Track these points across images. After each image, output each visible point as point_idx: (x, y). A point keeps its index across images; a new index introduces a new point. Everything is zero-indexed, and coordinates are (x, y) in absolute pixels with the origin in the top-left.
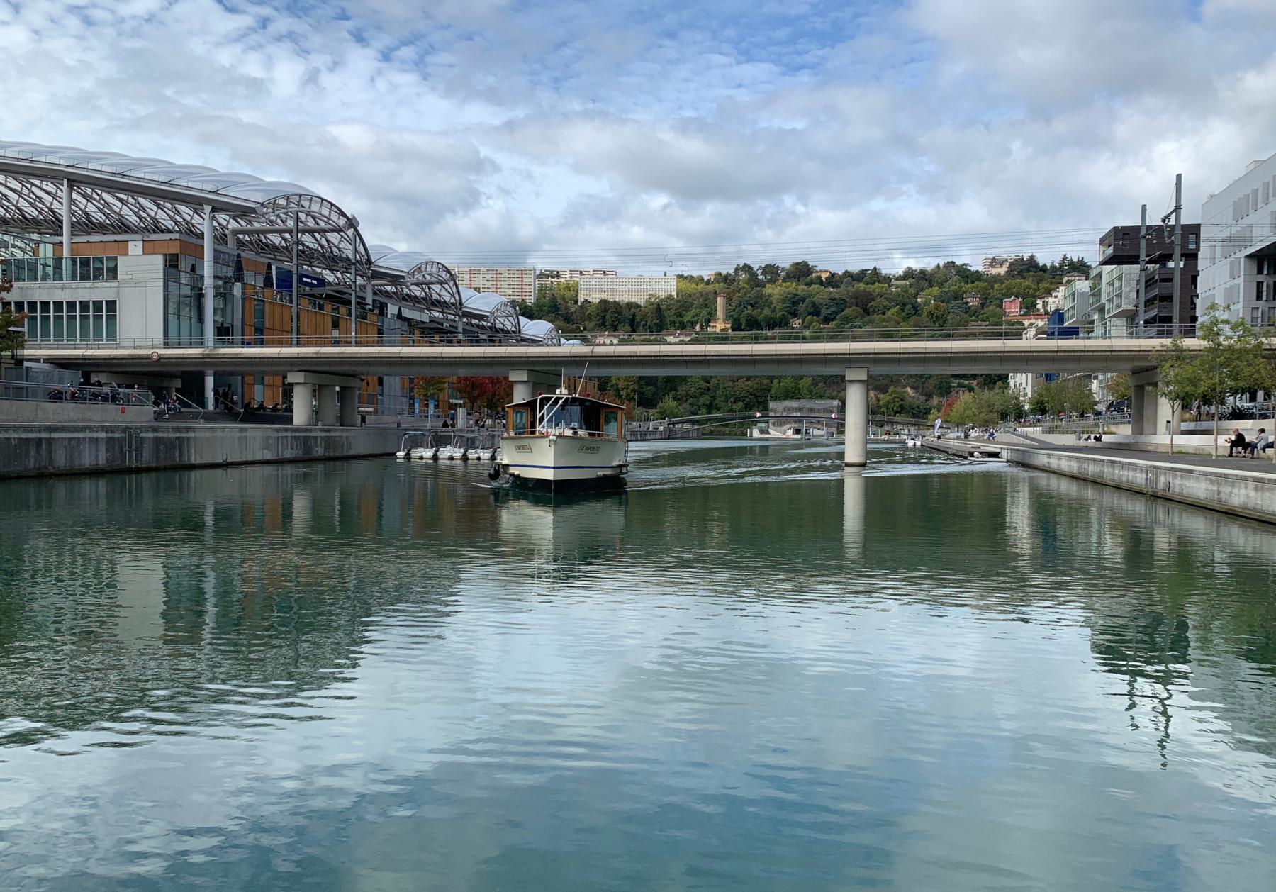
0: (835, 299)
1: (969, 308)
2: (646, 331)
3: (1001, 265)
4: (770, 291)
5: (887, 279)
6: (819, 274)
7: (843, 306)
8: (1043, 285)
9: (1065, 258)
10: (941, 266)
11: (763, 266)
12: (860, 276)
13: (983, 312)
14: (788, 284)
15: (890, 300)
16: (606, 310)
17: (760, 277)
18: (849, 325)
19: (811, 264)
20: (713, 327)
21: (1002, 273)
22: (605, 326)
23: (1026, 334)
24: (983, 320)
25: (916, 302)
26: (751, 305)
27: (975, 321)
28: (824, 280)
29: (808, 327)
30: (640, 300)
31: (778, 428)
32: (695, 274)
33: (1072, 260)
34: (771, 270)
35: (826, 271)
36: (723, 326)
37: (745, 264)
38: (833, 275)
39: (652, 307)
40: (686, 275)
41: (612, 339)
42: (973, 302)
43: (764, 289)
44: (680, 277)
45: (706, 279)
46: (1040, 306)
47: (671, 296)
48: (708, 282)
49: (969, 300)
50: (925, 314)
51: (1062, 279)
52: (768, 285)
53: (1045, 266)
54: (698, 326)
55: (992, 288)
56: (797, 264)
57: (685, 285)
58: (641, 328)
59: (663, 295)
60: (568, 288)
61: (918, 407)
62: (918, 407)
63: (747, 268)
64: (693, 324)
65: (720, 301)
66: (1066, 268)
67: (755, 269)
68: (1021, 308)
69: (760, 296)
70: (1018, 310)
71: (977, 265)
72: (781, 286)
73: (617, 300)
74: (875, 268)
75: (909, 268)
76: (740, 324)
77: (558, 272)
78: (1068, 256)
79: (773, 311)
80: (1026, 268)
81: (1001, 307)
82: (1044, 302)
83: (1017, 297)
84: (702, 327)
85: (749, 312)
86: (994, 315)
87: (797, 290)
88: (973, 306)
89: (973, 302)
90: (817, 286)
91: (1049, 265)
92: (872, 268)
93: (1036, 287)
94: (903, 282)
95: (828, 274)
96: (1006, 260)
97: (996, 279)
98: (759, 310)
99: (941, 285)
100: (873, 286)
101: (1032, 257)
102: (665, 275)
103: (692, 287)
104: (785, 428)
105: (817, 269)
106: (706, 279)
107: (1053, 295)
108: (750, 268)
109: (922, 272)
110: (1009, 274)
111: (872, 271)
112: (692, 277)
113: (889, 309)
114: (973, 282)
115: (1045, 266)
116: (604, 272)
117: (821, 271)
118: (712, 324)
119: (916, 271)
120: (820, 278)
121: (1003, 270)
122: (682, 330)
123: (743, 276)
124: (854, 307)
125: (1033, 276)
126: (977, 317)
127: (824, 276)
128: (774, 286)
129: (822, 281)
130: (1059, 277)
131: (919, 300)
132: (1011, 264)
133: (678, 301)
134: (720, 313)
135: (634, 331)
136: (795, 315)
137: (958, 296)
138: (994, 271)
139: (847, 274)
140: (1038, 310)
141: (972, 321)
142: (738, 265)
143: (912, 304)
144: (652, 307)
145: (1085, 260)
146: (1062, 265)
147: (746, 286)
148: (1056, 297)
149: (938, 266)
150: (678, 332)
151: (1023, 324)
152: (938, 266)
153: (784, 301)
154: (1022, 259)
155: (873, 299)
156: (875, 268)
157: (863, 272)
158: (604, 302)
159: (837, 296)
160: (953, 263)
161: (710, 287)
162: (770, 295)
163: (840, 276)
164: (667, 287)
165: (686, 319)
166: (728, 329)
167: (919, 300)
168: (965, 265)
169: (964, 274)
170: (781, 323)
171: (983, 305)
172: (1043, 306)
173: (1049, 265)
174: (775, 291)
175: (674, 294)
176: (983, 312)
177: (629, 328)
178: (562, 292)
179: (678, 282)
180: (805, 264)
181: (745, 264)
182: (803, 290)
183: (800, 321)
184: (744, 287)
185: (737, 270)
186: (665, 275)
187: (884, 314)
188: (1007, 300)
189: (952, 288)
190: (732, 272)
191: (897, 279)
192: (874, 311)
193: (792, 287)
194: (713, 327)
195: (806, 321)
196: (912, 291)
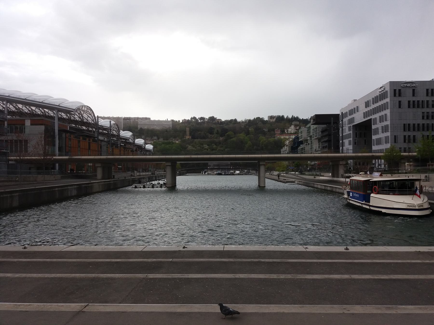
10: (255, 118)
11: (200, 117)
20: (185, 137)
21: (274, 121)
23: (286, 142)
28: (220, 122)
31: (212, 171)
36: (188, 137)
37: (194, 117)
46: (286, 131)
63: (194, 118)
67: (197, 118)
71: (266, 119)
80: (280, 119)
82: (287, 130)
83: (279, 129)
104: (214, 171)
108: (196, 118)
110: (276, 121)
121: (274, 120)
132: (277, 118)
138: (272, 120)
142: (192, 117)
145: (299, 117)
150: (174, 139)
168: (262, 118)
175: (171, 126)
180: (213, 117)
181: (194, 117)
185: (191, 118)
188: (276, 129)
190: (190, 119)
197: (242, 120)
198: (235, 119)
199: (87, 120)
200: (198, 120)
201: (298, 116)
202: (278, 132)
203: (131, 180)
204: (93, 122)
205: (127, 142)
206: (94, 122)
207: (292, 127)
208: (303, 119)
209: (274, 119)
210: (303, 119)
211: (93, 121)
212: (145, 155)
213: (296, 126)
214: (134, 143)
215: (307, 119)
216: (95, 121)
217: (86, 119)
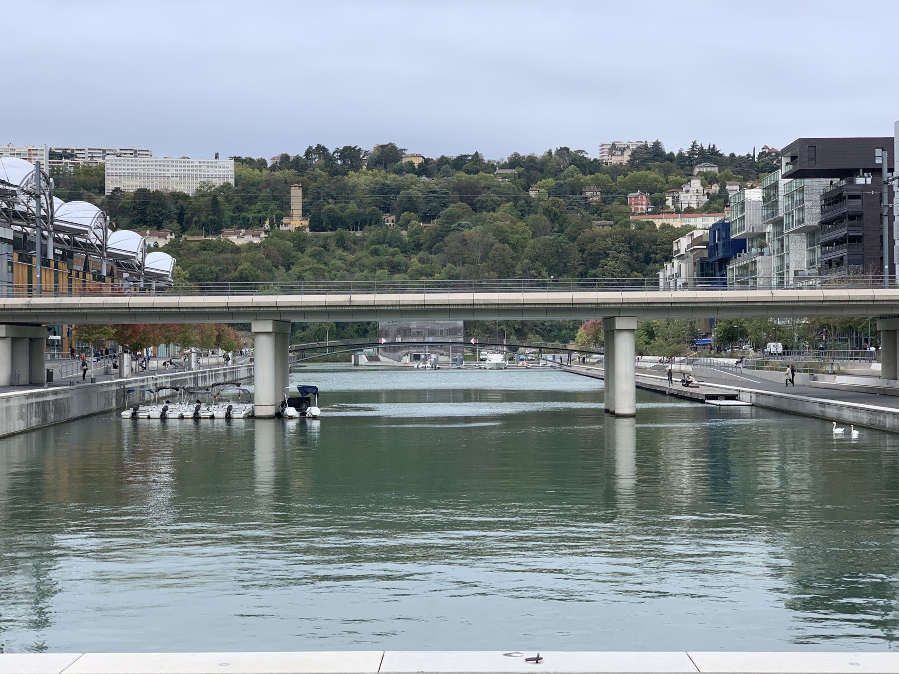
0: (435, 192)
1: (589, 204)
3: (622, 151)
5: (491, 167)
6: (410, 159)
7: (445, 201)
8: (671, 178)
9: (694, 145)
12: (460, 163)
13: (606, 208)
14: (376, 171)
15: (500, 194)
16: (146, 203)
17: (339, 162)
18: (454, 226)
19: (399, 147)
20: (286, 224)
21: (625, 162)
22: (145, 223)
24: (606, 219)
25: (529, 196)
26: (332, 197)
27: (598, 220)
28: (416, 166)
29: (405, 226)
30: (188, 188)
32: (255, 158)
33: (702, 148)
34: (350, 154)
35: (418, 156)
37: (319, 146)
38: (427, 161)
39: (206, 199)
40: (244, 158)
41: (156, 239)
42: (594, 196)
43: (346, 177)
44: (237, 159)
46: (669, 202)
47: (229, 184)
48: (273, 168)
50: (540, 210)
51: (692, 170)
52: (351, 173)
53: (672, 154)
54: (267, 223)
55: (614, 180)
56: (383, 147)
57: (246, 171)
58: (193, 225)
59: (218, 183)
60: (88, 171)
61: (543, 324)
62: (543, 324)
63: (321, 150)
64: (261, 222)
66: (696, 157)
67: (331, 151)
68: (648, 204)
69: (342, 188)
70: (645, 207)
71: (593, 154)
72: (365, 173)
73: (158, 188)
74: (477, 153)
75: (516, 154)
76: (321, 221)
77: (73, 150)
78: (698, 143)
79: (359, 206)
81: (626, 204)
82: (673, 197)
84: (272, 224)
86: (620, 213)
87: (386, 178)
88: (594, 201)
89: (594, 196)
90: (411, 175)
91: (676, 153)
92: (473, 153)
93: (663, 180)
94: (509, 171)
95: (421, 160)
96: (628, 147)
97: (617, 170)
99: (555, 174)
100: (476, 176)
101: (657, 145)
102: (217, 157)
105: (407, 153)
107: (684, 189)
109: (532, 159)
111: (473, 157)
112: (251, 160)
113: (499, 205)
114: (591, 173)
115: (672, 154)
116: (136, 151)
117: (412, 156)
118: (284, 221)
119: (524, 157)
120: (411, 164)
121: (625, 158)
122: (247, 228)
123: (316, 160)
124: (460, 203)
125: (659, 167)
126: (600, 215)
127: (417, 162)
128: (357, 173)
129: (414, 168)
130: (689, 168)
131: (533, 194)
132: (635, 152)
133: (238, 191)
135: (184, 230)
136: (387, 209)
137: (577, 189)
138: (616, 160)
139: (443, 160)
141: (594, 220)
143: (524, 199)
145: (718, 148)
146: (692, 153)
147: (323, 173)
148: (687, 192)
149: (550, 152)
150: (243, 231)
151: (654, 225)
152: (550, 152)
153: (372, 192)
154: (646, 146)
155: (479, 193)
156: (477, 153)
157: (462, 159)
158: (142, 192)
159: (436, 188)
160: (567, 149)
161: (278, 174)
162: (355, 186)
163: (434, 162)
165: (250, 215)
166: (305, 227)
167: (533, 194)
168: (580, 151)
170: (371, 221)
171: (604, 201)
172: (673, 203)
173: (676, 153)
175: (232, 181)
176: (606, 208)
177: (176, 225)
178: (82, 178)
179: (236, 166)
181: (319, 146)
182: (395, 180)
183: (393, 217)
184: (320, 176)
185: (309, 152)
186: (217, 157)
187: (494, 210)
189: (569, 179)
191: (503, 167)
193: (381, 176)
194: (286, 224)
195: (401, 218)
196: (522, 181)
197: (503, 159)
198: (477, 153)
200: (337, 160)
201: (714, 146)
202: (639, 203)
203: (114, 388)
205: (76, 244)
207: (696, 184)
208: (733, 155)
209: (622, 154)
210: (733, 155)
212: (143, 291)
213: (708, 180)
214: (103, 247)
215: (749, 155)
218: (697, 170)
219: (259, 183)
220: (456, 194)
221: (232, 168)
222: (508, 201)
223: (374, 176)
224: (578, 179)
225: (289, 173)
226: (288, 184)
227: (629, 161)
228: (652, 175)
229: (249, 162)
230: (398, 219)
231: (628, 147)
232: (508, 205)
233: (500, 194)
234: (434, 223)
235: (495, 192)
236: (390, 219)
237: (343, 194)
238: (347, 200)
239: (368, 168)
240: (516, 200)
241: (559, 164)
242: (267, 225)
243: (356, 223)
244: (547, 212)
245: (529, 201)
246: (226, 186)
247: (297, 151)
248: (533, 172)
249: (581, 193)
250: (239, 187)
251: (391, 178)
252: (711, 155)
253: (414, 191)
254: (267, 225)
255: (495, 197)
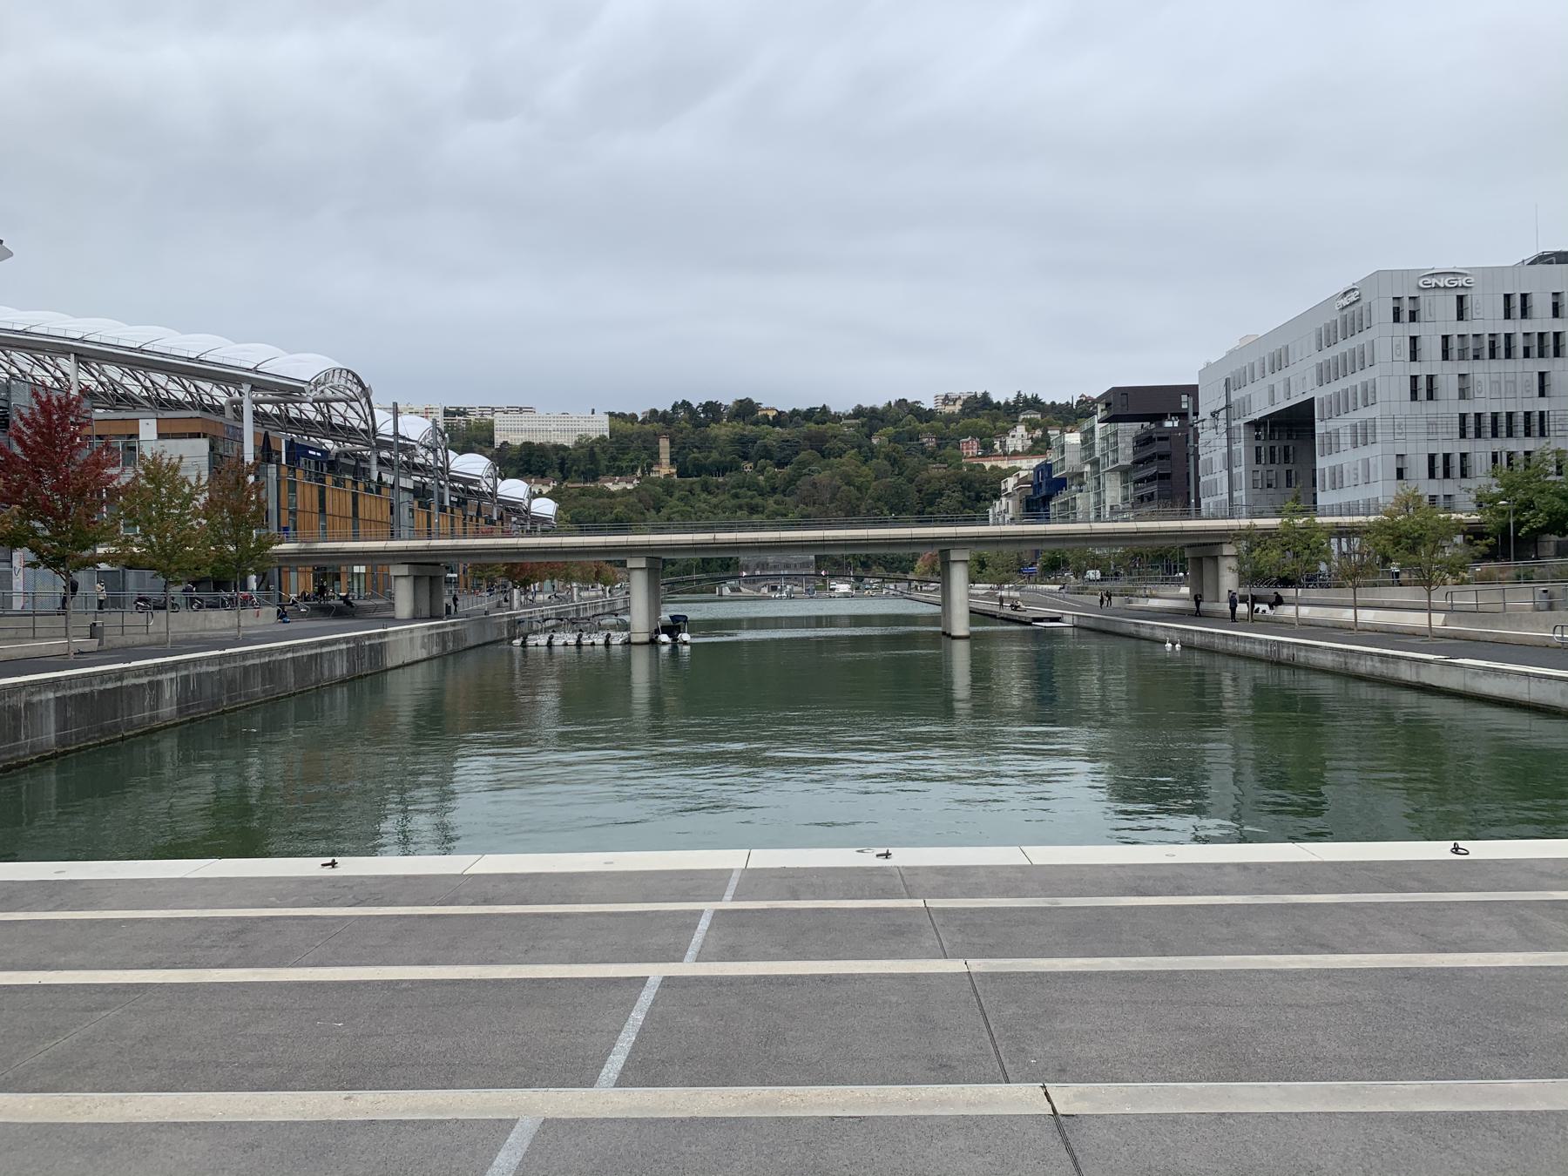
2: (579, 476)
3: (955, 401)
4: (716, 431)
5: (837, 418)
7: (796, 449)
8: (999, 424)
9: (1019, 395)
12: (809, 414)
13: (941, 453)
15: (845, 442)
17: (702, 415)
19: (756, 401)
21: (957, 411)
26: (696, 447)
28: (771, 418)
29: (761, 472)
30: (568, 441)
32: (627, 413)
34: (712, 408)
35: (773, 409)
37: (684, 401)
38: (780, 413)
39: (584, 450)
41: (540, 486)
42: (929, 442)
44: (611, 414)
45: (640, 419)
46: (997, 446)
47: (605, 436)
48: (644, 422)
49: (925, 440)
51: (1017, 417)
52: (713, 425)
53: (999, 403)
54: (639, 471)
55: (948, 427)
56: (741, 401)
57: (620, 425)
59: (595, 435)
63: (686, 405)
64: (634, 470)
65: (664, 444)
67: (695, 406)
69: (706, 439)
70: (975, 451)
71: (928, 404)
72: (725, 426)
75: (859, 406)
76: (687, 469)
79: (720, 454)
80: (980, 405)
85: (696, 455)
86: (952, 457)
87: (744, 430)
89: (929, 442)
90: (766, 426)
91: (1002, 402)
92: (821, 406)
93: (992, 426)
94: (853, 421)
95: (775, 413)
96: (960, 398)
97: (950, 418)
98: (706, 453)
99: (895, 423)
100: (824, 426)
101: (985, 395)
102: (593, 413)
103: (628, 427)
105: (762, 406)
106: (640, 419)
108: (689, 405)
109: (873, 410)
111: (821, 409)
115: (999, 403)
117: (767, 409)
118: (654, 469)
120: (767, 416)
121: (957, 408)
126: (935, 459)
127: (771, 414)
129: (769, 420)
130: (1014, 415)
131: (875, 441)
132: (965, 402)
134: (665, 457)
135: (565, 478)
136: (746, 457)
137: (914, 436)
138: (949, 409)
139: (795, 412)
140: (996, 451)
144: (584, 450)
145: (1040, 397)
146: (1017, 401)
148: (1013, 436)
153: (732, 442)
154: (975, 396)
155: (827, 441)
157: (811, 411)
159: (789, 438)
160: (905, 400)
161: (647, 427)
162: (716, 437)
164: (599, 427)
165: (624, 465)
167: (875, 441)
169: (915, 411)
171: (938, 446)
173: (1002, 402)
174: (722, 431)
175: (607, 434)
176: (941, 453)
177: (558, 474)
180: (749, 401)
181: (684, 401)
183: (751, 464)
184: (685, 428)
185: (675, 407)
186: (593, 413)
187: (840, 457)
189: (907, 428)
190: (669, 409)
191: (848, 417)
192: (829, 453)
193: (739, 427)
196: (866, 430)
199: (345, 419)
204: (363, 426)
206: (367, 424)
211: (366, 422)
213: (1031, 426)
216: (370, 422)
217: (341, 416)
218: (1022, 417)
219: (631, 435)
220: (808, 443)
221: (607, 422)
222: (853, 448)
223: (734, 427)
224: (914, 427)
225: (658, 426)
226: (657, 436)
227: (960, 410)
228: (982, 422)
229: (622, 416)
230: (755, 466)
231: (960, 398)
232: (853, 452)
233: (845, 442)
234: (788, 469)
235: (840, 440)
236: (749, 465)
237: (705, 444)
238: (710, 449)
239: (728, 421)
240: (859, 447)
241: (898, 414)
242: (639, 473)
243: (718, 470)
244: (887, 457)
245: (871, 449)
246: (602, 438)
247: (665, 406)
248: (875, 422)
249: (918, 440)
250: (614, 439)
251: (749, 429)
252: (1034, 404)
253: (769, 441)
254: (639, 473)
255: (841, 445)
